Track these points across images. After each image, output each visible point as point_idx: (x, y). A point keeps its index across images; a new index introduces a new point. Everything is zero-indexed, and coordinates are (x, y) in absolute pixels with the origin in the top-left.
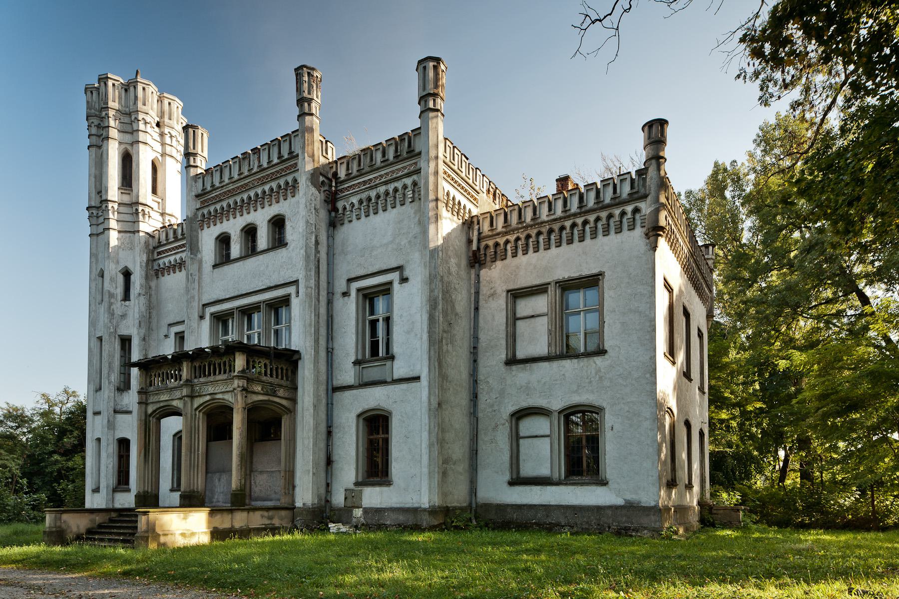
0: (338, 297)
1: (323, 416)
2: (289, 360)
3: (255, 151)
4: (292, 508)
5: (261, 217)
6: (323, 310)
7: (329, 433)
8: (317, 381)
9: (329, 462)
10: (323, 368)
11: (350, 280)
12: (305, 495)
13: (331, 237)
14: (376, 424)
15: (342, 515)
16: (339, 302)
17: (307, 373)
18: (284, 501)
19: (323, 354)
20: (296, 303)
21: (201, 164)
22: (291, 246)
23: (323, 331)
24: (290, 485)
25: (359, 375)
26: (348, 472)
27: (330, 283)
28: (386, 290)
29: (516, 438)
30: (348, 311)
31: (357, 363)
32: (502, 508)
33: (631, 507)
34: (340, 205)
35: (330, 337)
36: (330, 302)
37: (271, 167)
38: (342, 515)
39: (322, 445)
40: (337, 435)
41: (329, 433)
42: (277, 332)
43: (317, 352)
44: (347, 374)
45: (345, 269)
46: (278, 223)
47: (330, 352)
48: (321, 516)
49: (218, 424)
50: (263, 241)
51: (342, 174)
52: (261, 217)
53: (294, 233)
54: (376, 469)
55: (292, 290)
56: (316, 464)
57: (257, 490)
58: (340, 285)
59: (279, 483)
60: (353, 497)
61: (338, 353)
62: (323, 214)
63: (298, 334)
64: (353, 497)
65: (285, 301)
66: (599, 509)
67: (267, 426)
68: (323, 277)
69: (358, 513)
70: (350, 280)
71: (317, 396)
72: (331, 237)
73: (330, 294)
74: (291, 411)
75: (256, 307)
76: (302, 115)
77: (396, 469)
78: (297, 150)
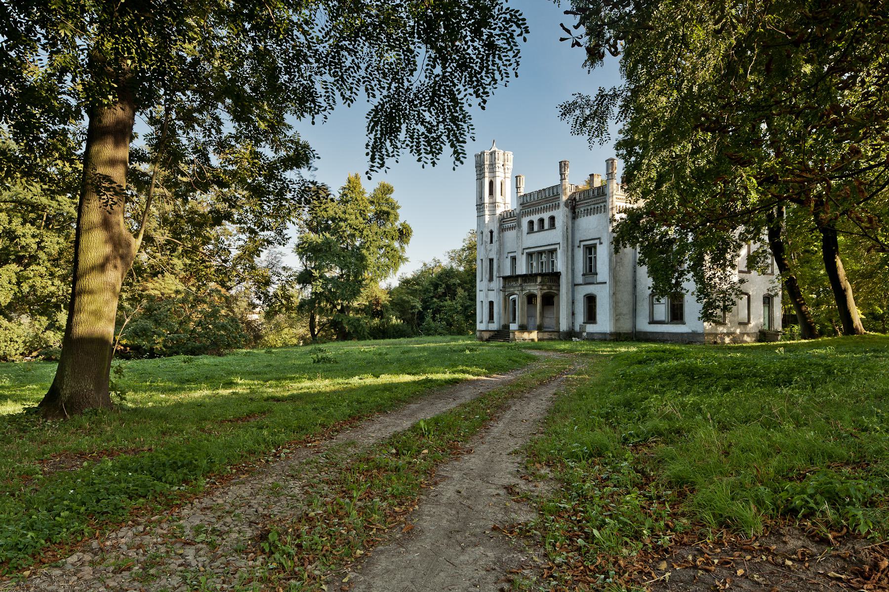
0: (576, 248)
1: (570, 296)
2: (558, 275)
3: (544, 190)
4: (558, 332)
5: (546, 216)
6: (570, 253)
7: (573, 303)
8: (568, 283)
9: (573, 314)
10: (570, 276)
11: (581, 241)
12: (564, 327)
13: (573, 223)
14: (591, 300)
15: (578, 335)
16: (576, 249)
17: (563, 281)
18: (556, 329)
19: (570, 271)
20: (559, 251)
21: (522, 192)
22: (558, 228)
23: (570, 262)
24: (558, 323)
25: (584, 280)
26: (580, 318)
27: (573, 242)
28: (595, 246)
29: (652, 305)
30: (580, 254)
31: (583, 275)
32: (645, 333)
33: (694, 334)
34: (577, 210)
35: (573, 264)
36: (573, 250)
37: (548, 198)
38: (578, 335)
39: (570, 307)
40: (576, 303)
41: (573, 303)
42: (553, 262)
43: (567, 272)
44: (579, 279)
45: (579, 236)
46: (552, 219)
47: (573, 270)
48: (570, 335)
49: (531, 298)
50: (546, 226)
51: (577, 198)
52: (546, 216)
53: (559, 223)
54: (591, 317)
55: (557, 246)
56: (568, 315)
57: (545, 324)
58: (577, 243)
59: (554, 322)
60: (583, 329)
61: (576, 270)
62: (570, 215)
63: (560, 265)
64: (583, 329)
65: (555, 250)
66: (682, 334)
67: (549, 300)
68: (570, 240)
69: (585, 334)
70: (581, 241)
71: (568, 289)
72: (573, 223)
73: (573, 246)
74: (558, 295)
75: (544, 251)
76: (561, 180)
77: (598, 317)
78: (560, 192)
